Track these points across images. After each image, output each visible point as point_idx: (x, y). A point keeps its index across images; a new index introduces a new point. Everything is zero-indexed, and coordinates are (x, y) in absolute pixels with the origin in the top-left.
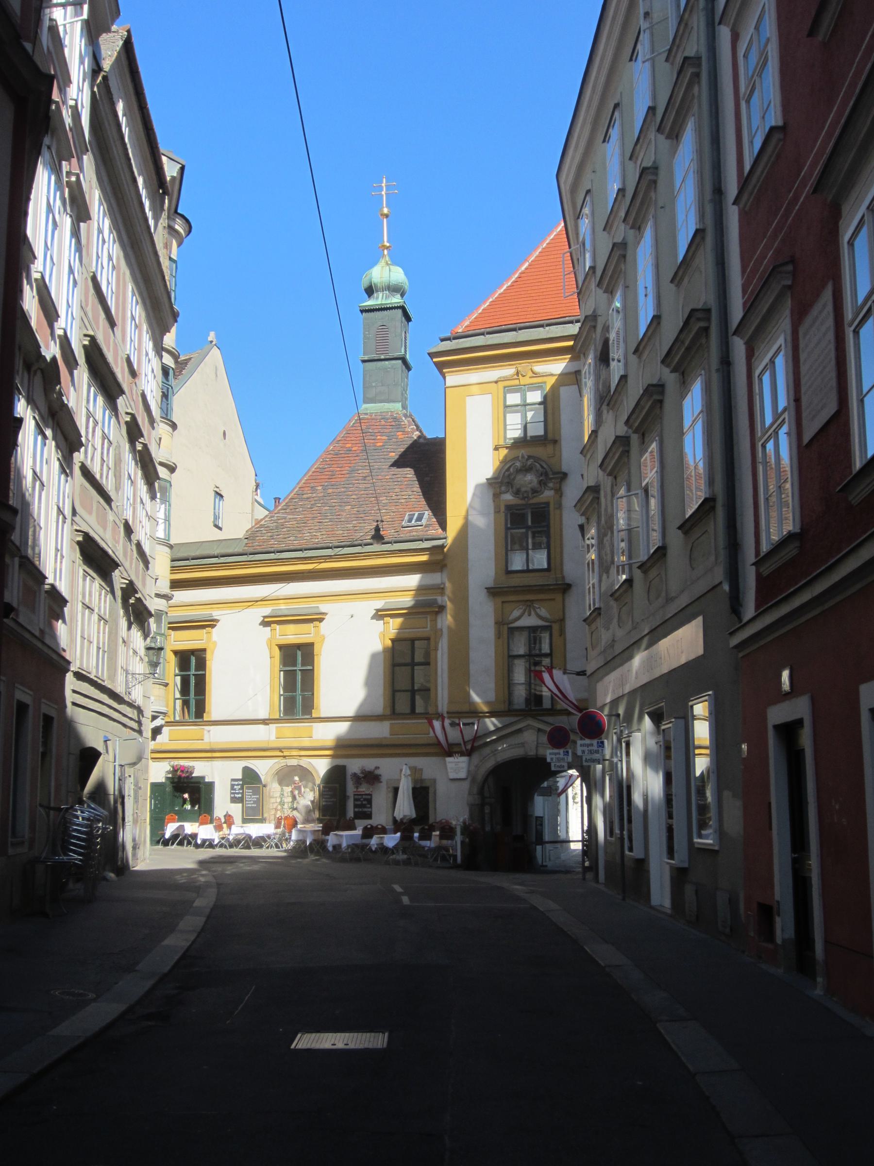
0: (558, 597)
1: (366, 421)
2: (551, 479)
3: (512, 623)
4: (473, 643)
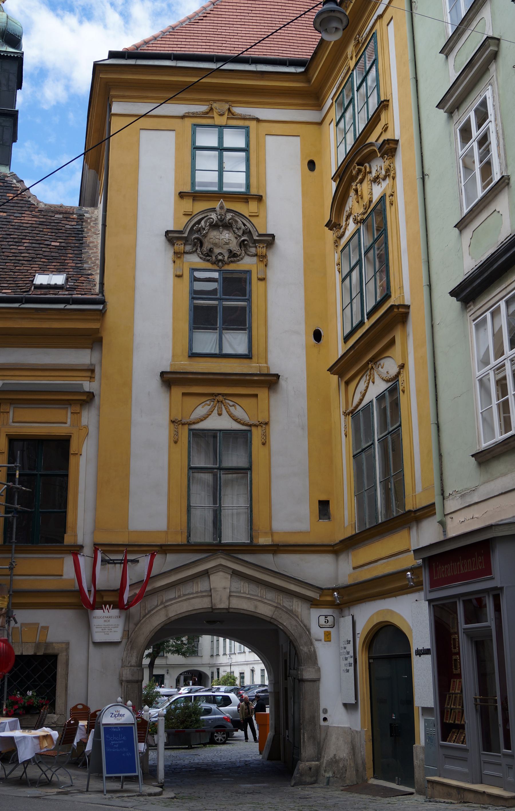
0: (263, 393)
2: (255, 242)
3: (194, 423)
4: (136, 448)
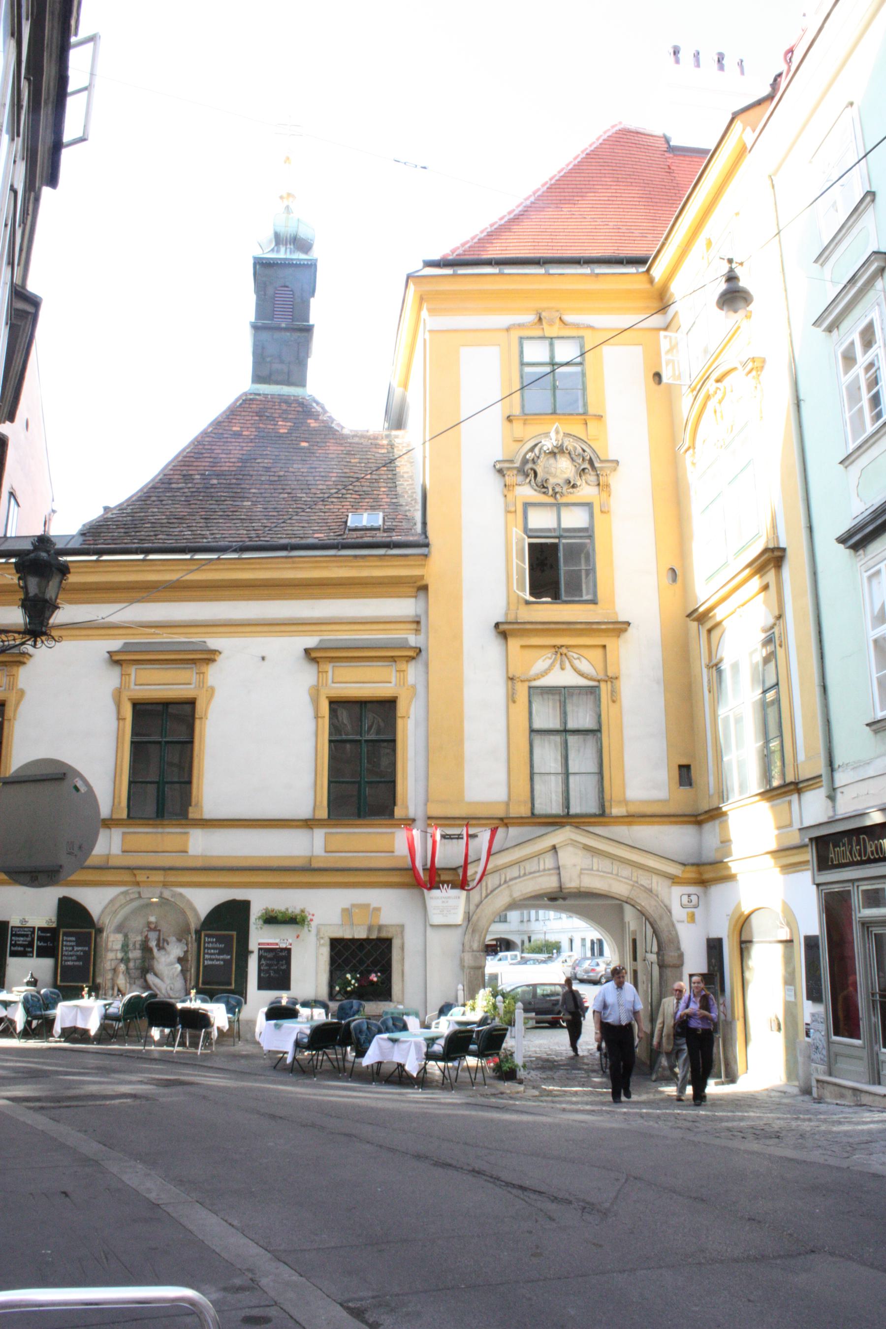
1: (259, 402)
4: (470, 709)
